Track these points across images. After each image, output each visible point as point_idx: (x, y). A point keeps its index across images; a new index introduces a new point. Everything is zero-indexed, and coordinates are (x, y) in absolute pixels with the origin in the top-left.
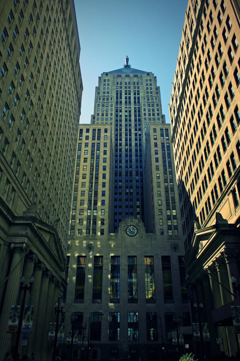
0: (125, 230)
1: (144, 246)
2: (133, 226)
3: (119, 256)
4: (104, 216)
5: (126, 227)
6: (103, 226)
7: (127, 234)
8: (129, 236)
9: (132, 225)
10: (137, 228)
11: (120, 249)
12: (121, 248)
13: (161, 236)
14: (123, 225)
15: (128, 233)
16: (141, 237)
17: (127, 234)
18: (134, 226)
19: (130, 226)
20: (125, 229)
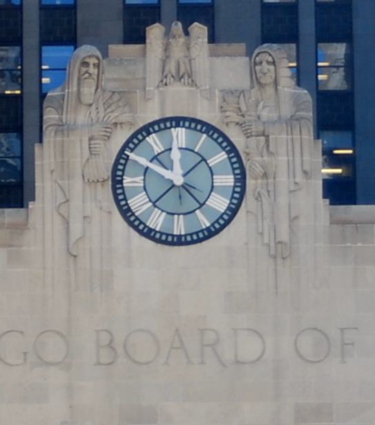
1: (307, 344)
7: (126, 212)
8: (148, 233)
9: (178, 121)
10: (232, 150)
14: (82, 117)
15: (139, 203)
16: (281, 252)
17: (126, 212)
18: (209, 129)
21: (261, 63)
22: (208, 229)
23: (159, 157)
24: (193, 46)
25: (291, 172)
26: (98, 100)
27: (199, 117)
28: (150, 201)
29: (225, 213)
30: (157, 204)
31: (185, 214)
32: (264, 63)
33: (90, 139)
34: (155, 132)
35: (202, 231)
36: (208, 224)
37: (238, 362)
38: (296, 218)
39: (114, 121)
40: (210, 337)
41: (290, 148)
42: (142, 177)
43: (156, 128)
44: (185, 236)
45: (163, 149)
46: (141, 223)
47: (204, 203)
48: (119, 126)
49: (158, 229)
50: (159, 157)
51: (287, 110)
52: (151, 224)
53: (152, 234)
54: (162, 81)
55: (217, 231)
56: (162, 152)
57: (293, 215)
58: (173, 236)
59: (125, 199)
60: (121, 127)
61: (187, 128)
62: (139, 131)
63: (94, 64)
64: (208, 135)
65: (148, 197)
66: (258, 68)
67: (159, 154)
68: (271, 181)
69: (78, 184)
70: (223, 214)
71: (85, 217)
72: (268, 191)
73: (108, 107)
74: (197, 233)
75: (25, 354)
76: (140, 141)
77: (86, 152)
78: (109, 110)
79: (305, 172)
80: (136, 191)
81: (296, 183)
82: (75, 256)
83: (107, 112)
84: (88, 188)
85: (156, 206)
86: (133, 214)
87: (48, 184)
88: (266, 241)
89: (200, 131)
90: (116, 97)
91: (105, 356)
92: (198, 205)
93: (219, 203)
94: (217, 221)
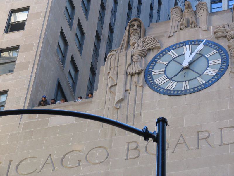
24: (199, 13)
39: (148, 47)
40: (203, 135)
48: (151, 51)
52: (167, 87)
56: (178, 57)
60: (153, 51)
63: (138, 26)
65: (167, 76)
69: (122, 76)
71: (126, 91)
77: (129, 61)
78: (146, 43)
80: (159, 75)
83: (144, 45)
84: (129, 77)
91: (132, 154)
93: (211, 72)
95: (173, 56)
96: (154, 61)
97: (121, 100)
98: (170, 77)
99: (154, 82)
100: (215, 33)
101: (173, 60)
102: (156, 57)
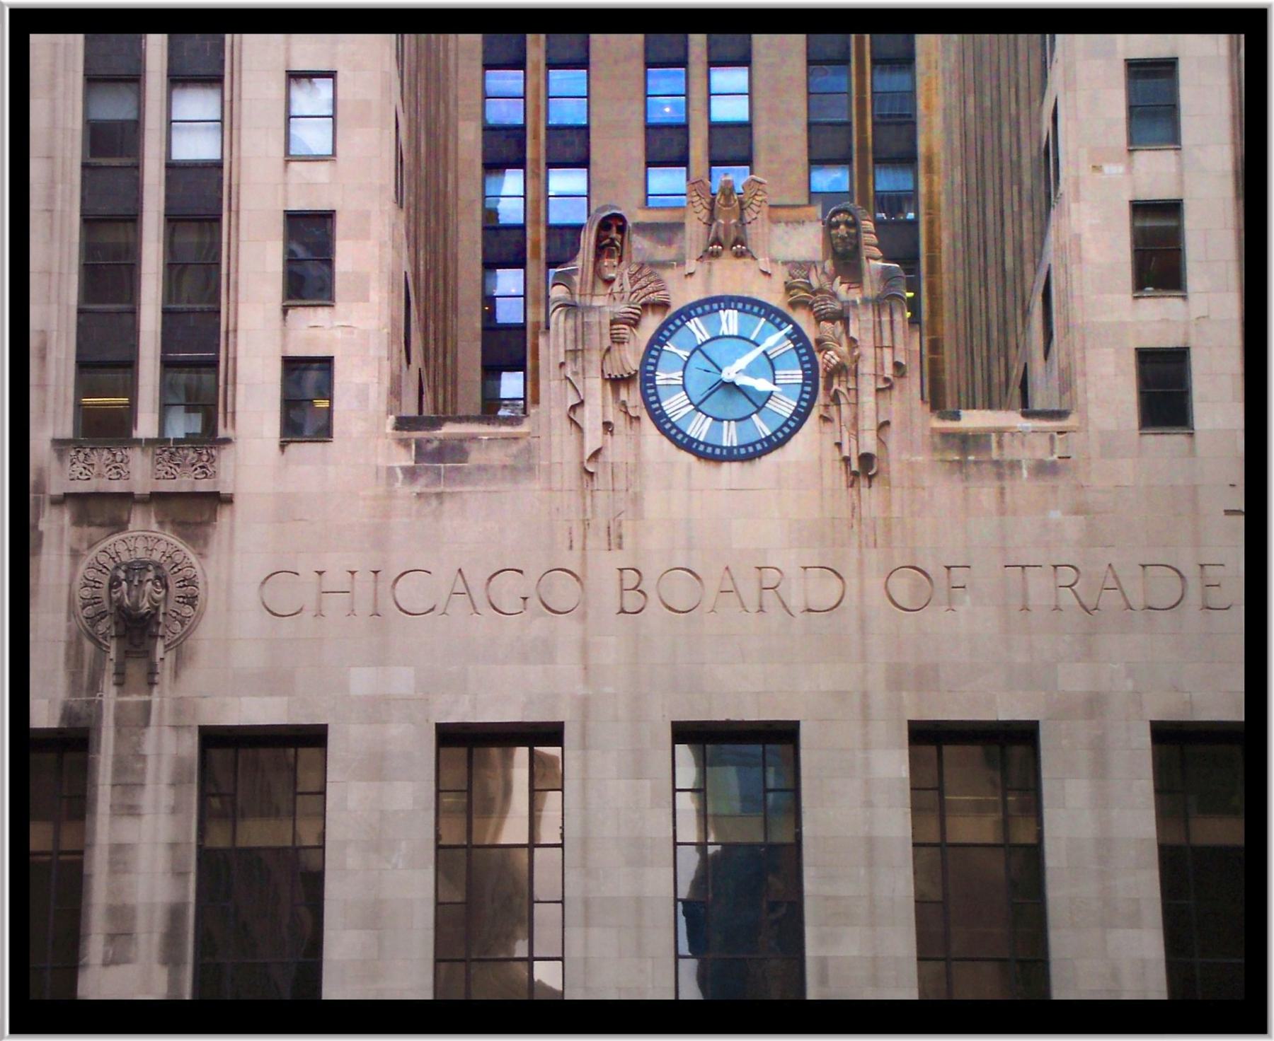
0: (633, 364)
1: (902, 587)
2: (748, 305)
3: (552, 734)
4: (321, 172)
5: (652, 323)
6: (321, 315)
7: (660, 419)
8: (688, 445)
11: (568, 628)
12: (580, 611)
13: (1151, 440)
15: (675, 405)
16: (865, 468)
17: (660, 419)
19: (711, 305)
20: (630, 358)
21: (837, 225)
22: (768, 439)
23: (703, 348)
25: (879, 365)
26: (622, 275)
27: (756, 296)
28: (691, 403)
29: (791, 419)
30: (701, 407)
31: (736, 420)
32: (842, 227)
33: (613, 323)
34: (698, 316)
35: (760, 441)
36: (768, 433)
37: (809, 610)
38: (887, 423)
40: (771, 577)
41: (877, 334)
42: (681, 373)
43: (699, 310)
44: (739, 447)
45: (708, 337)
46: (680, 431)
47: (763, 406)
49: (701, 439)
50: (703, 348)
51: (871, 287)
52: (692, 431)
53: (695, 445)
54: (706, 251)
55: (782, 443)
56: (708, 341)
57: (881, 420)
58: (722, 448)
59: (658, 401)
61: (739, 311)
62: (678, 314)
64: (768, 320)
66: (834, 232)
67: (703, 343)
68: (851, 378)
70: (788, 419)
72: (849, 390)
73: (636, 282)
74: (753, 445)
75: (525, 599)
76: (678, 328)
77: (607, 342)
78: (637, 286)
79: (897, 366)
81: (886, 380)
82: (591, 474)
85: (699, 410)
86: (669, 420)
87: (555, 384)
88: (846, 453)
89: (758, 315)
90: (646, 271)
91: (632, 601)
92: (755, 409)
93: (784, 407)
94: (780, 429)
95: (701, 337)
96: (657, 342)
97: (596, 454)
98: (696, 402)
99: (661, 408)
100: (789, 288)
101: (698, 348)
102: (659, 332)
